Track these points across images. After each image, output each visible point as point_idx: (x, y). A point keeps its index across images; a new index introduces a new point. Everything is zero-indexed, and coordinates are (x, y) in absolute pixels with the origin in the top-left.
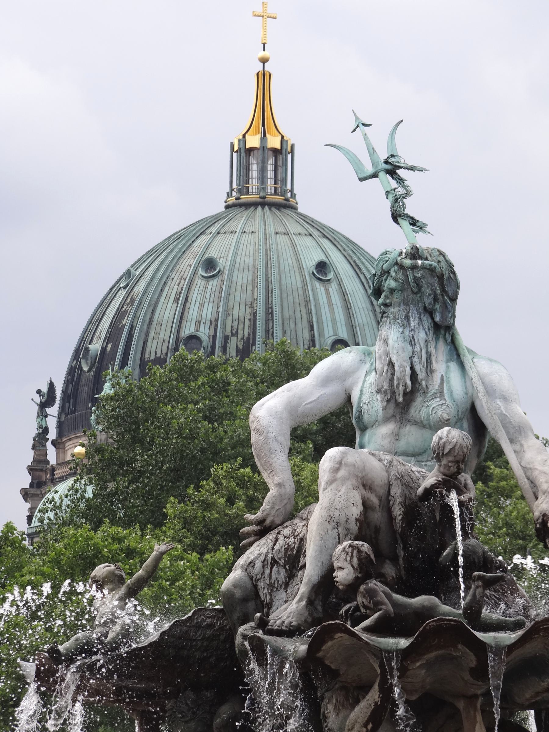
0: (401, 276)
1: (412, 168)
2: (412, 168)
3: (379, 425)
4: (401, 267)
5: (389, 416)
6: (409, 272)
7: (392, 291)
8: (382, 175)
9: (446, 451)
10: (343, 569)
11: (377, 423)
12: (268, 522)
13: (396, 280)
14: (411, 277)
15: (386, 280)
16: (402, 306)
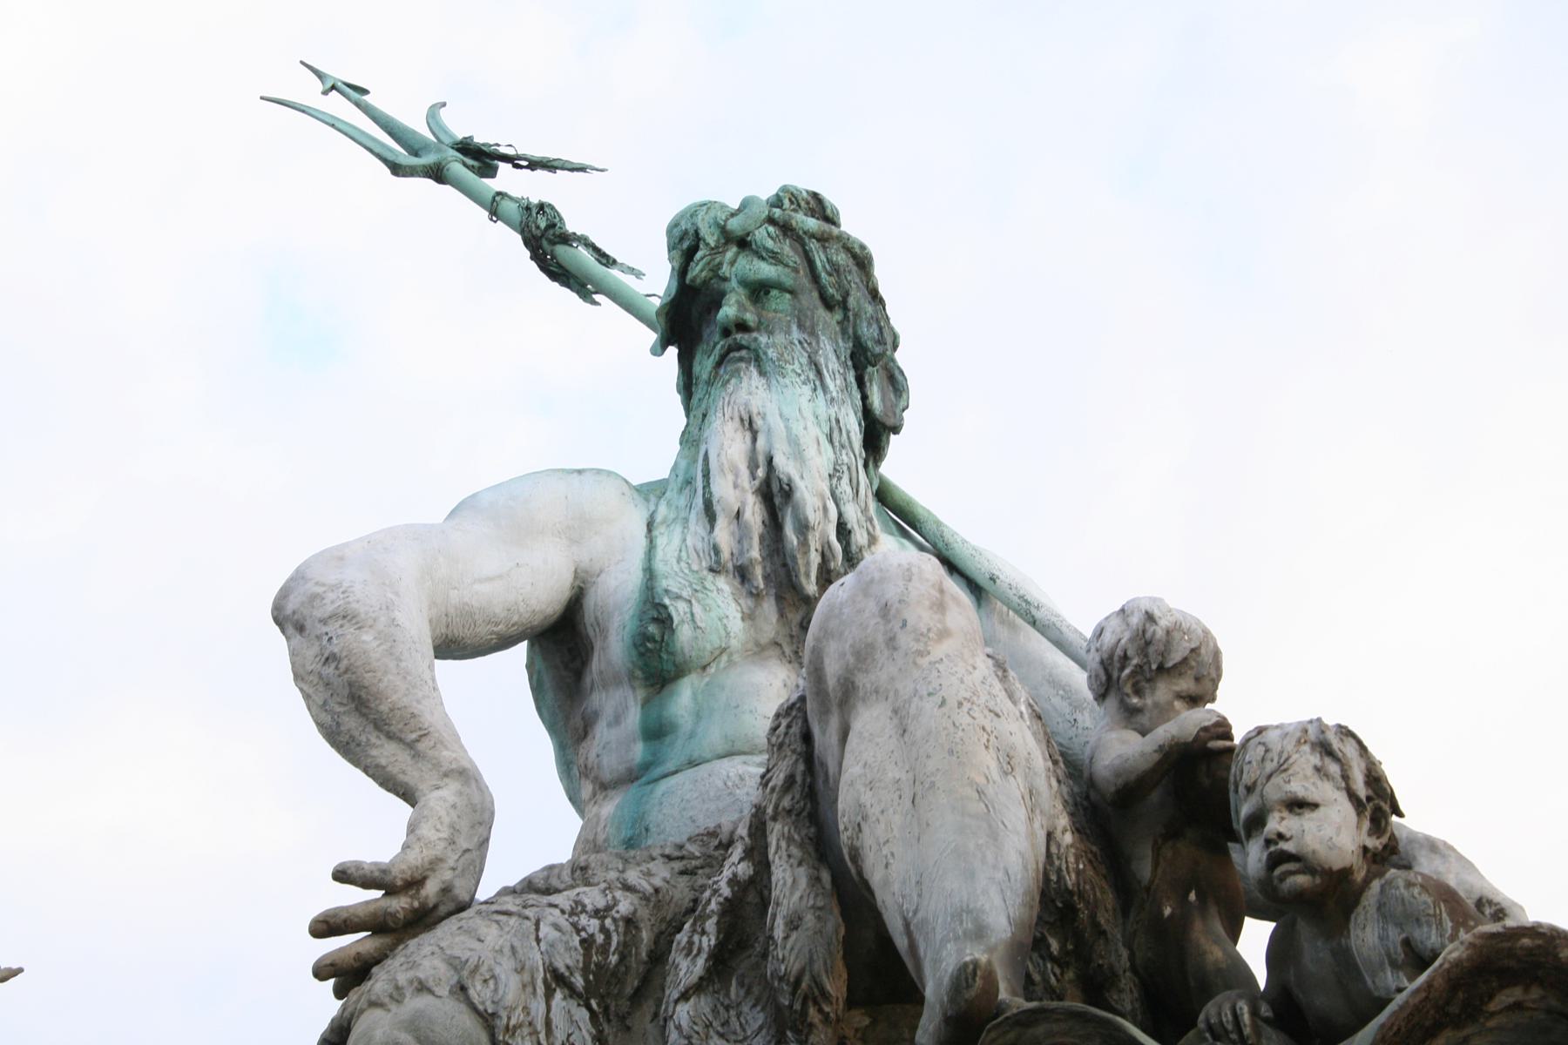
0: (787, 249)
1: (548, 165)
2: (548, 165)
3: (731, 662)
4: (786, 229)
5: (764, 641)
6: (813, 245)
7: (758, 291)
8: (457, 168)
9: (1176, 657)
10: (1315, 806)
11: (724, 658)
12: (431, 889)
13: (775, 258)
14: (819, 259)
15: (732, 263)
16: (796, 334)
